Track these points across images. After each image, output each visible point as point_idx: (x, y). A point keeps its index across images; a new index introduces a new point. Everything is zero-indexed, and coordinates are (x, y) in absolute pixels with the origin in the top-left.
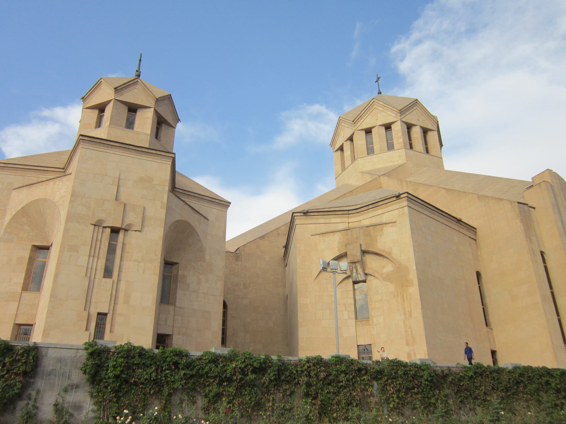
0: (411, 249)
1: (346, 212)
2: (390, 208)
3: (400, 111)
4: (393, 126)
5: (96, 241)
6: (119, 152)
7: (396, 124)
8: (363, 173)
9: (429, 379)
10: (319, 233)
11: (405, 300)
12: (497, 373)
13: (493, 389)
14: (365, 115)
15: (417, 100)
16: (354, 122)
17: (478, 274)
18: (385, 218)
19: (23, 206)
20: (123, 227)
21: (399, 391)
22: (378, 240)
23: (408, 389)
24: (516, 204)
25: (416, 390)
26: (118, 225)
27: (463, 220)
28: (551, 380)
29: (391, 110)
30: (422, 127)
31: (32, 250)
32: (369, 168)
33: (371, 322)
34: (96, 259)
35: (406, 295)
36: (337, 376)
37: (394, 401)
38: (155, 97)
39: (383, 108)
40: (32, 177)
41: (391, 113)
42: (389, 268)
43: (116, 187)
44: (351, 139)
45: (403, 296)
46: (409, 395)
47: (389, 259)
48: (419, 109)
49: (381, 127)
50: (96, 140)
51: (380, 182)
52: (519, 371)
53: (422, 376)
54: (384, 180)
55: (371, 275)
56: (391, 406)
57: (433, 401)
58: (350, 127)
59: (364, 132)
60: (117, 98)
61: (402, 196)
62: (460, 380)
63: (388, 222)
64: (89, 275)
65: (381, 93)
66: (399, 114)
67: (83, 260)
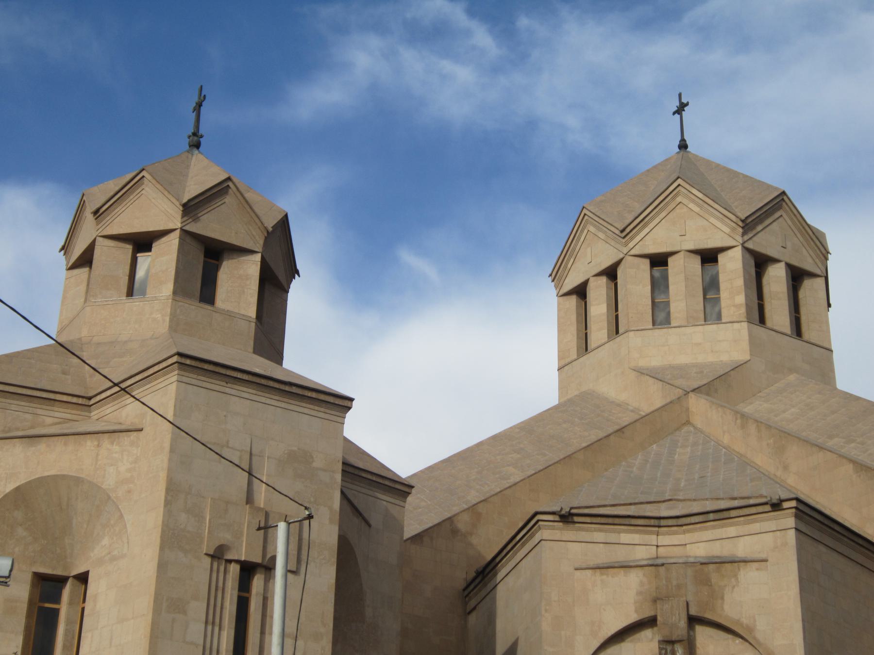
0: (798, 626)
1: (652, 522)
2: (756, 527)
4: (721, 258)
5: (216, 590)
6: (248, 392)
7: (730, 253)
8: (640, 372)
10: (592, 564)
15: (784, 193)
16: (625, 233)
18: (743, 548)
19: (18, 484)
20: (265, 563)
22: (726, 597)
26: (256, 558)
29: (721, 216)
30: (790, 267)
31: (33, 585)
32: (655, 361)
34: (217, 629)
38: (266, 228)
41: (719, 224)
44: (611, 273)
49: (692, 255)
50: (206, 366)
51: (688, 409)
54: (698, 405)
58: (613, 243)
59: (647, 262)
60: (187, 228)
61: (786, 505)
63: (749, 558)
66: (741, 230)
67: (196, 630)
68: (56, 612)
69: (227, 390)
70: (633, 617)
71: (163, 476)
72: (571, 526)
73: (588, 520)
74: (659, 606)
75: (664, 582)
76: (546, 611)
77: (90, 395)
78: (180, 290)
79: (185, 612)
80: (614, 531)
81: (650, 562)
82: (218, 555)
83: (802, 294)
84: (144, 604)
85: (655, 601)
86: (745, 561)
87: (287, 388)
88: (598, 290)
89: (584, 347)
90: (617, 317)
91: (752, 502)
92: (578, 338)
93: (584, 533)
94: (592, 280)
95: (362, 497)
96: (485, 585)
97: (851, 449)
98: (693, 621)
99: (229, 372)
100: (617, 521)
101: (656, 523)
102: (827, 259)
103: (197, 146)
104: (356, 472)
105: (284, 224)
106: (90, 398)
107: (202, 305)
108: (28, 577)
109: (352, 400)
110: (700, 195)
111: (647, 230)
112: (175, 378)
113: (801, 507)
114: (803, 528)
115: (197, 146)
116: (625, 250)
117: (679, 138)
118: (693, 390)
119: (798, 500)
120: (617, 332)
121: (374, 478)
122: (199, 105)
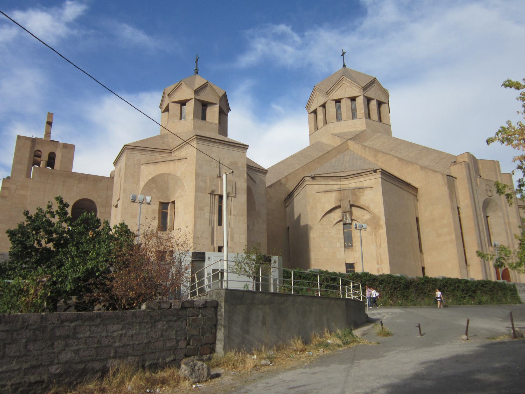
0: (382, 206)
1: (339, 178)
2: (369, 178)
3: (363, 88)
6: (217, 145)
7: (359, 97)
8: (334, 135)
9: (405, 284)
10: (321, 191)
11: (377, 237)
12: (435, 281)
13: (433, 289)
14: (335, 89)
15: (375, 78)
16: (327, 93)
17: (417, 219)
18: (365, 184)
19: (152, 177)
21: (391, 289)
22: (361, 199)
23: (395, 289)
24: (446, 176)
25: (399, 289)
27: (411, 184)
28: (460, 285)
30: (378, 101)
31: (159, 205)
32: (338, 131)
33: (354, 250)
34: (213, 215)
35: (378, 234)
36: (365, 282)
37: (389, 294)
38: (219, 97)
39: (350, 84)
40: (152, 157)
41: (356, 89)
42: (367, 216)
43: (219, 169)
44: (324, 106)
45: (376, 235)
46: (395, 291)
47: (367, 211)
48: (376, 86)
49: (348, 99)
50: (204, 138)
51: (348, 145)
52: (445, 281)
53: (401, 283)
54: (351, 144)
55: (355, 220)
56: (387, 296)
57: (406, 294)
59: (334, 102)
60: (196, 98)
61: (378, 171)
62: (418, 285)
64: (211, 224)
65: (345, 66)
66: (362, 90)
67: (207, 215)
68: (167, 213)
69: (211, 145)
70: (334, 206)
71: (194, 171)
72: (315, 180)
73: (320, 178)
74: (341, 202)
75: (343, 195)
76: (309, 205)
77: (171, 149)
78: (195, 116)
79: (204, 210)
80: (327, 181)
81: (338, 190)
82: (212, 193)
83: (381, 109)
84: (192, 209)
85: (340, 201)
86: (366, 188)
87: (229, 144)
88: (320, 111)
89: (317, 128)
90: (326, 119)
91: (368, 170)
92: (315, 126)
93: (319, 182)
94: (318, 108)
95: (253, 175)
96: (291, 199)
97: (397, 154)
98: (351, 206)
99: (211, 140)
100: (328, 178)
101: (340, 178)
102: (389, 98)
103: (197, 73)
104: (251, 168)
105: (225, 95)
106: (171, 150)
107: (202, 121)
108: (158, 203)
109: (248, 146)
110: (350, 80)
111: (334, 92)
112: (196, 142)
113: (383, 171)
114: (383, 177)
115: (197, 73)
116: (328, 98)
117: (343, 63)
118: (349, 139)
119: (381, 169)
120: (326, 123)
121: (256, 169)
122: (197, 60)
